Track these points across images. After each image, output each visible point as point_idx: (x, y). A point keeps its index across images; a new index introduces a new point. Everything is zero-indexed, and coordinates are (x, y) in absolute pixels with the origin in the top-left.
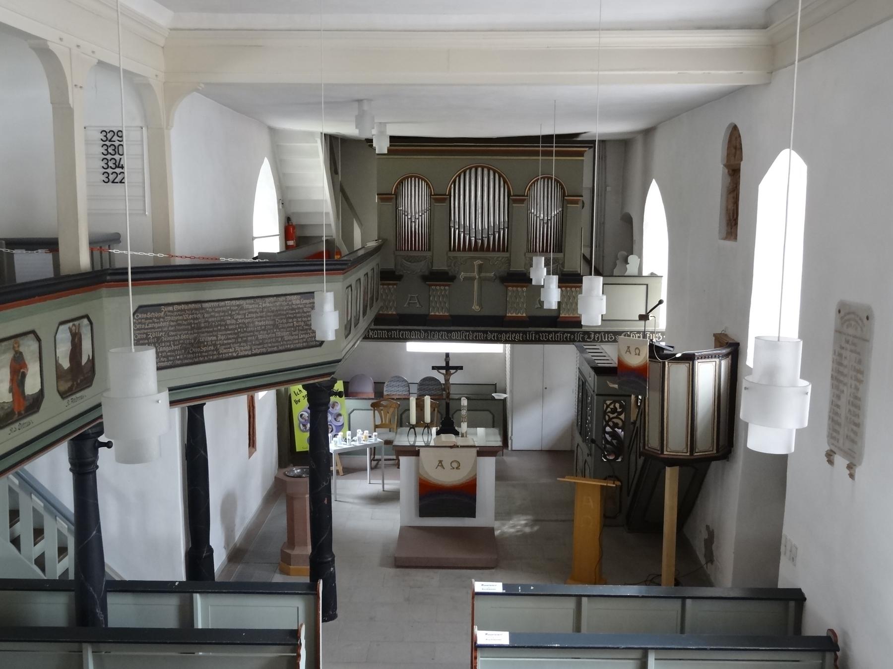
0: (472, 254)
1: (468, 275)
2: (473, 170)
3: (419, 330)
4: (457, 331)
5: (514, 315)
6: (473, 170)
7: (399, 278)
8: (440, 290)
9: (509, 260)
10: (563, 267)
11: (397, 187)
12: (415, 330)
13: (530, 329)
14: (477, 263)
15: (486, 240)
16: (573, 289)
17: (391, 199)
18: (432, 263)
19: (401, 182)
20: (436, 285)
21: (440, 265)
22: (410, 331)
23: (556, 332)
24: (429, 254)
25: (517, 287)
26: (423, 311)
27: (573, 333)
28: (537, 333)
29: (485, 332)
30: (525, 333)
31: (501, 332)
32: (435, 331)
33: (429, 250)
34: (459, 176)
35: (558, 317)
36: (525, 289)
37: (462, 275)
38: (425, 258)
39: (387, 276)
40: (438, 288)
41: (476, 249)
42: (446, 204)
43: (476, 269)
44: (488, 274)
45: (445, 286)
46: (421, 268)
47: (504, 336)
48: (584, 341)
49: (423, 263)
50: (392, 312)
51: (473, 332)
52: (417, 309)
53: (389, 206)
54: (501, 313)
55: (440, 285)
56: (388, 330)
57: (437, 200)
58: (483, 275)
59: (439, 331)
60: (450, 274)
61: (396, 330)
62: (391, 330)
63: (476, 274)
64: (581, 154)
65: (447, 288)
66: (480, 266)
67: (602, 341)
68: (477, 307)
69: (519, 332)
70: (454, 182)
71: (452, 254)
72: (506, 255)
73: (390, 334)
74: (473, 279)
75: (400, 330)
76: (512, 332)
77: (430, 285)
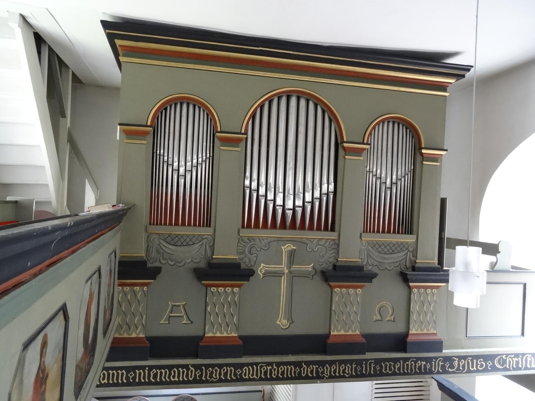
0: (278, 234)
1: (273, 267)
2: (284, 101)
3: (186, 367)
4: (252, 364)
5: (342, 333)
6: (284, 101)
7: (153, 273)
8: (224, 293)
9: (337, 245)
10: (415, 256)
11: (156, 117)
12: (178, 366)
13: (369, 355)
14: (286, 248)
15: (299, 211)
16: (429, 291)
17: (146, 133)
18: (212, 248)
19: (164, 108)
20: (217, 286)
21: (226, 252)
22: (170, 367)
23: (406, 360)
24: (206, 232)
25: (347, 287)
26: (193, 331)
27: (428, 360)
28: (378, 361)
29: (298, 364)
30: (359, 362)
31: (322, 364)
32: (213, 366)
33: (209, 225)
34: (262, 106)
35: (407, 335)
36: (359, 291)
37: (261, 269)
38: (201, 238)
39: (132, 270)
40: (221, 290)
41: (283, 226)
42: (240, 149)
43: (285, 259)
44: (303, 268)
45: (232, 286)
46: (194, 255)
47: (327, 371)
48: (445, 372)
49: (196, 246)
50: (138, 334)
51: (278, 364)
52: (182, 328)
53: (145, 143)
54: (320, 330)
55: (225, 286)
56: (128, 369)
57: (227, 141)
58: (295, 267)
59: (220, 366)
60: (243, 266)
61: (143, 368)
62: (134, 368)
63: (284, 267)
64: (442, 87)
65: (236, 290)
66: (292, 254)
67: (469, 371)
68: (285, 322)
69: (351, 362)
70: (253, 116)
71: (246, 233)
72: (333, 236)
73: (131, 375)
74: (278, 275)
75: (151, 368)
76: (341, 362)
77: (207, 286)
